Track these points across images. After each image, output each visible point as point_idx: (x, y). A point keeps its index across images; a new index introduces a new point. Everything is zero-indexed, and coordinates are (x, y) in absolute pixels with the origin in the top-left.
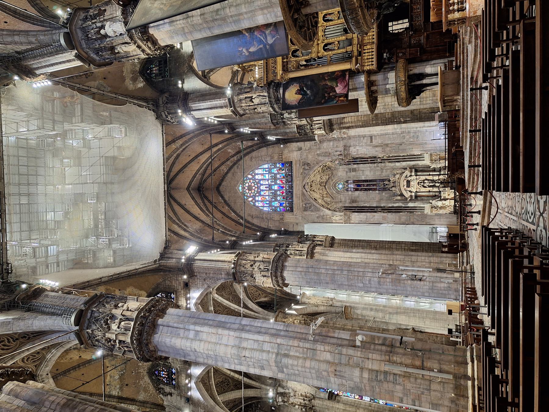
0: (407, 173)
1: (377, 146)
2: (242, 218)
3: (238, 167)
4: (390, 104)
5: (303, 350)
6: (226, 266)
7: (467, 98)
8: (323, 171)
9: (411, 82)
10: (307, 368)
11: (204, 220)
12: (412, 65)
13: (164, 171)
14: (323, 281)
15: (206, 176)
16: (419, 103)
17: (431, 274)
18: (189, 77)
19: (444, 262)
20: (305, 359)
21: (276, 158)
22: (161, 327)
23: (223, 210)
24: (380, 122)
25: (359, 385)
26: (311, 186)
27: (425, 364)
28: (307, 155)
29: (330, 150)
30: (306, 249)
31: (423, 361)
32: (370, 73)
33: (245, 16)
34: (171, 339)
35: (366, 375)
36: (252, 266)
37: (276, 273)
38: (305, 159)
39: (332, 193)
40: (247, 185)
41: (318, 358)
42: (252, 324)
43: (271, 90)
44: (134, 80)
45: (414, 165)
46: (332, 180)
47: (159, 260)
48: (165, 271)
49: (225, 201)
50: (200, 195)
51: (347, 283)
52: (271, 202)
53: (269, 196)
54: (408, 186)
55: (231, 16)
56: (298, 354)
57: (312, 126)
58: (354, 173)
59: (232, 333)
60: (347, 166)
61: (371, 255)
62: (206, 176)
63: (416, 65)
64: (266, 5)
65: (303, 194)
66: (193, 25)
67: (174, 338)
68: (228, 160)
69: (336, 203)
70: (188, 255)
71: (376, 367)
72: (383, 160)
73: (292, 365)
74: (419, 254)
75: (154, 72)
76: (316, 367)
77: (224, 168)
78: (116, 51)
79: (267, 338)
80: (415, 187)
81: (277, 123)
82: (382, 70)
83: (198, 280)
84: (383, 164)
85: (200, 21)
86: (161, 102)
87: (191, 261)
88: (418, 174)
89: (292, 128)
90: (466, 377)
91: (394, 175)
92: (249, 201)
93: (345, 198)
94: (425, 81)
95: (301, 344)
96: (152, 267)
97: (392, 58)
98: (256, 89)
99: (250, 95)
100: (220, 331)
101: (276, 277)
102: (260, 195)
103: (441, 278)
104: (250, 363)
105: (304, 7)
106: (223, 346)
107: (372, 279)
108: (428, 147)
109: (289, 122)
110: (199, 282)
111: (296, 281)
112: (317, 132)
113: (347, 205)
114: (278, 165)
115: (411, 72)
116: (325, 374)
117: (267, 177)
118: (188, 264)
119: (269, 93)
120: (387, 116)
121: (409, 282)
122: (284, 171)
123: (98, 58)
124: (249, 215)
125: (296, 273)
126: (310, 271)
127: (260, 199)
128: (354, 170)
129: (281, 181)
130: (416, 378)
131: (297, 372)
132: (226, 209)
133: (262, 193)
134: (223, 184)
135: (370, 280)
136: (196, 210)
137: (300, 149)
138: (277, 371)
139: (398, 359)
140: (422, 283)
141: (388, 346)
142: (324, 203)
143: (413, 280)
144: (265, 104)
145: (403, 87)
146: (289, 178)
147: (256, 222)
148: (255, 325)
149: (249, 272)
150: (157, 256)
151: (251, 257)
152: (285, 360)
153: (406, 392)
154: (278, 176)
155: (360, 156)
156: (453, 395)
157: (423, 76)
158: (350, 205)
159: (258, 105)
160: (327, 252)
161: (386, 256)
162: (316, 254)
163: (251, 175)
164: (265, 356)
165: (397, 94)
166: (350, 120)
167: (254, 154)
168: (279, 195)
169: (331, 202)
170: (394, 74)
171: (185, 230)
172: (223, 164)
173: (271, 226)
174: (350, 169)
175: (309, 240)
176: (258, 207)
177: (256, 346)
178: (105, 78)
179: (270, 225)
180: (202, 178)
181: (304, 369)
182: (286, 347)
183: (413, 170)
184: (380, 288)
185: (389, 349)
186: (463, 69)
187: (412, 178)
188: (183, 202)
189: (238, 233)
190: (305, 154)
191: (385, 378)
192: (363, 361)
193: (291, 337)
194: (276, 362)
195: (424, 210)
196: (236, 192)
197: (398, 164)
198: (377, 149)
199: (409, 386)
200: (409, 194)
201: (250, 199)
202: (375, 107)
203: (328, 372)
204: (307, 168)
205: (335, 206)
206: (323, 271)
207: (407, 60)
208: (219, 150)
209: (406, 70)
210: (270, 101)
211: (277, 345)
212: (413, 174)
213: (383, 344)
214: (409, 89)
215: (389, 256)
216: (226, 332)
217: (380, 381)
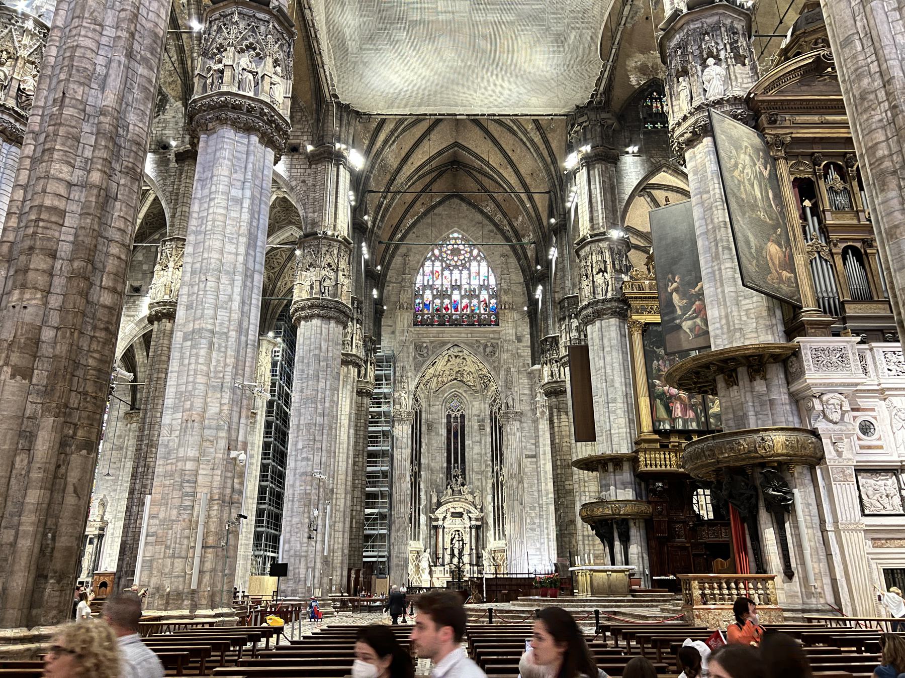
0: (475, 513)
1: (520, 465)
2: (402, 238)
3: (492, 231)
4: (587, 489)
5: (221, 372)
6: (328, 220)
7: (587, 606)
8: (481, 377)
9: (617, 523)
10: (195, 378)
11: (402, 173)
12: (642, 525)
13: (489, 115)
14: (305, 384)
15: (479, 176)
16: (586, 533)
17: (319, 554)
18: (642, 165)
19: (335, 573)
20: (208, 375)
21: (505, 298)
22: (246, 141)
23: (418, 203)
24: (559, 471)
25: (173, 456)
26: (456, 357)
27: (210, 550)
28: (508, 351)
29: (516, 389)
30: (354, 352)
31: (213, 547)
32: (633, 460)
33: (719, 290)
34: (229, 159)
35: (189, 466)
36: (329, 265)
37: (318, 306)
38: (503, 347)
39: (444, 392)
40: (461, 247)
41: (210, 394)
42: (255, 291)
43: (615, 305)
44: (642, 69)
45: (487, 523)
46: (465, 391)
47: (338, 103)
48: (318, 111)
49: (433, 207)
50: (445, 165)
51: (302, 422)
52: (431, 287)
53: (442, 285)
54: (454, 515)
55: (720, 269)
56: (214, 363)
57: (556, 362)
58: (476, 427)
59: (241, 259)
60: (488, 417)
61: (345, 458)
62: (479, 176)
64: (731, 324)
65: (444, 344)
66: (711, 208)
67: (229, 163)
68: (504, 215)
69: (428, 398)
70: (345, 154)
71: (200, 479)
72: (496, 474)
73: (197, 356)
74: (347, 535)
75: (654, 105)
76: (197, 392)
77: (489, 208)
78: (681, 79)
79: (235, 316)
80: (452, 525)
81: (564, 307)
82: (638, 480)
83: (302, 171)
84: (490, 474)
85: (716, 221)
86: (604, 115)
87: (338, 159)
88: (473, 531)
89: (554, 329)
90: (194, 607)
91: (472, 493)
92: (433, 250)
93: (436, 413)
94: (617, 544)
95: (229, 369)
96: (326, 90)
97: (655, 494)
98: (618, 279)
99: (609, 269)
100: (243, 240)
101: (310, 307)
102: (443, 270)
103: (314, 569)
104: (196, 288)
105: (725, 379)
106: (221, 245)
107: (310, 463)
108: (516, 547)
109: (563, 327)
110: (298, 171)
111: (304, 339)
112: (546, 371)
113: (424, 415)
114: (493, 301)
115: (632, 524)
116: (188, 405)
117: (475, 283)
118: (331, 153)
119: (611, 300)
120: (567, 483)
121: (307, 520)
122: (482, 311)
123: (672, 45)
124: (409, 250)
125: (318, 340)
126: (322, 364)
127: (435, 269)
128: (482, 428)
129: (466, 307)
130: (188, 538)
131: (186, 362)
132: (420, 209)
133: (447, 273)
134: (464, 205)
135: (308, 459)
136: (419, 158)
137: (519, 339)
138: (185, 330)
139: (215, 512)
140: (305, 540)
141: (231, 497)
142: (427, 377)
143: (310, 526)
144: (594, 293)
145: (610, 512)
146: (473, 321)
147: (397, 261)
148: (254, 296)
149: (318, 262)
150: (344, 99)
151: (343, 265)
152: (204, 343)
153: (167, 524)
154: (475, 301)
155: (505, 438)
156: (168, 590)
157: (626, 541)
158: (423, 421)
159: (593, 282)
160: (349, 387)
161: (344, 481)
162: (346, 369)
163: (479, 255)
164: (209, 312)
165: (601, 502)
166: (563, 424)
167: (513, 260)
168: (442, 303)
169: (429, 390)
170: (631, 498)
171: (386, 142)
172: (498, 205)
173: (390, 288)
174: (483, 420)
175: (367, 355)
176: (423, 265)
177: (222, 298)
178: (647, 18)
179: (391, 285)
180: (474, 168)
181: (192, 373)
182: (223, 345)
183: (479, 523)
184: (295, 475)
185: (227, 499)
186: (629, 601)
187: (467, 521)
188: (433, 136)
189: (380, 233)
190: (510, 348)
191: (187, 494)
192: (209, 461)
193: (238, 352)
194: (201, 329)
195: (415, 539)
196: (448, 227)
197: (490, 498)
198: (515, 466)
199: (178, 527)
200: (441, 517)
201: (437, 252)
202: (581, 469)
203: (190, 410)
204: (488, 350)
205: (422, 396)
206: (321, 385)
207: (651, 518)
208: (522, 202)
209: (636, 517)
210: (598, 301)
211: (225, 330)
212: (474, 523)
213: (233, 490)
214: (606, 520)
215: (344, 487)
216: (242, 250)
217: (182, 487)
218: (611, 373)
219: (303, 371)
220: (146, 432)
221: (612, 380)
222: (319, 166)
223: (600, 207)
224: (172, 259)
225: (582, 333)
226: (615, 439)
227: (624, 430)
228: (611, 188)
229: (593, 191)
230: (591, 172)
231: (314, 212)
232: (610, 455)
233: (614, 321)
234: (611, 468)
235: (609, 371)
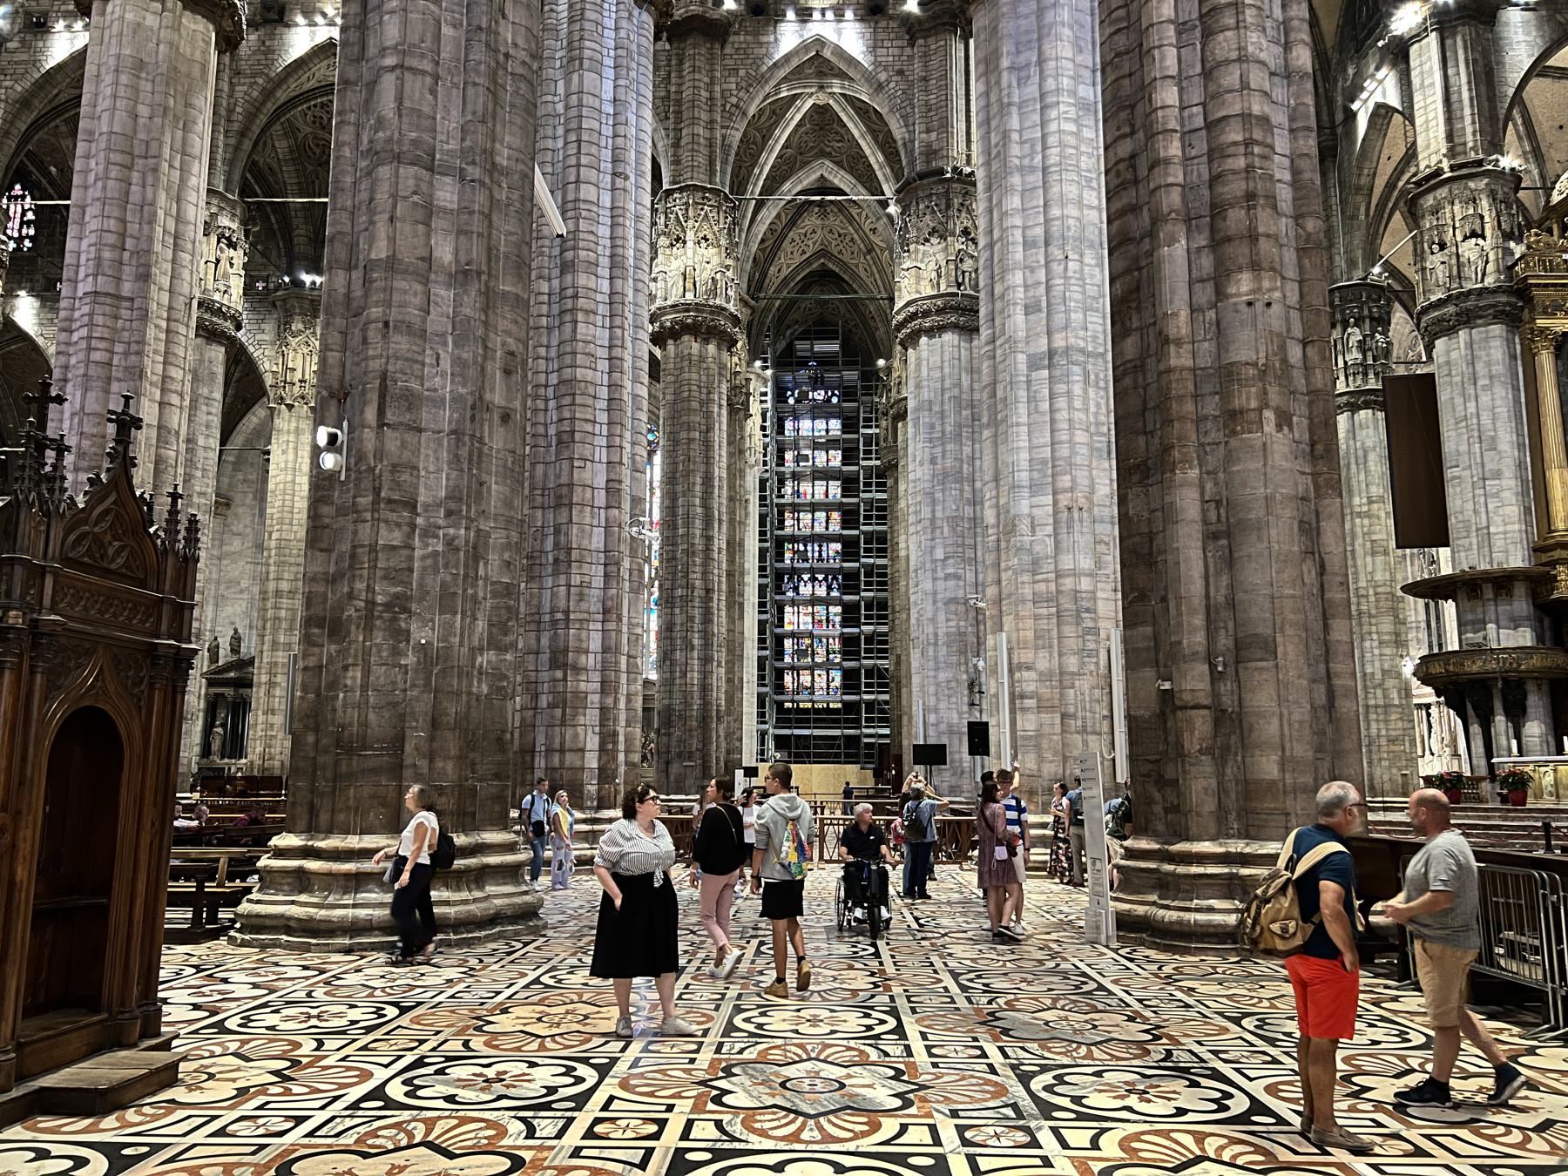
4: (1374, 629)
6: (958, 147)
10: (1072, 435)
12: (1545, 688)
16: (1372, 702)
37: (955, 309)
43: (1504, 299)
51: (939, 514)
56: (1093, 409)
63: (1547, 700)
83: (896, 52)
94: (1500, 722)
99: (1488, 233)
101: (940, 311)
110: (889, 53)
111: (929, 369)
121: (965, 677)
125: (956, 370)
126: (964, 413)
135: (957, 577)
138: (1032, 350)
140: (965, 708)
149: (950, 226)
157: (1517, 716)
159: (1458, 256)
184: (935, 602)
203: (1072, 490)
209: (1539, 676)
214: (1484, 681)
218: (1490, 427)
219: (932, 426)
220: (680, 531)
221: (1493, 438)
222: (931, 40)
223: (1467, 111)
224: (691, 223)
225: (1369, 354)
226: (1498, 543)
227: (1516, 527)
228: (1486, 71)
229: (1452, 80)
230: (1449, 42)
231: (928, 131)
232: (1485, 572)
233: (1497, 330)
234: (1488, 592)
235: (1486, 419)
